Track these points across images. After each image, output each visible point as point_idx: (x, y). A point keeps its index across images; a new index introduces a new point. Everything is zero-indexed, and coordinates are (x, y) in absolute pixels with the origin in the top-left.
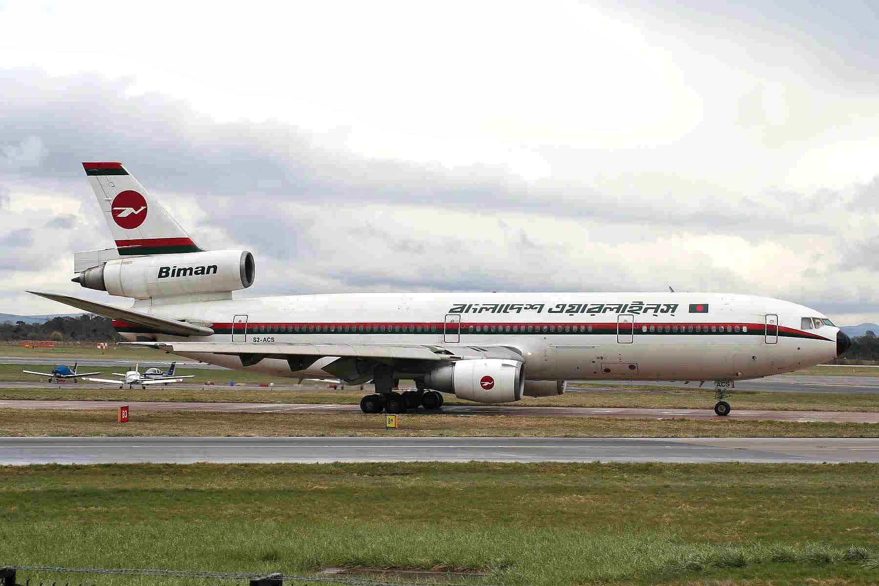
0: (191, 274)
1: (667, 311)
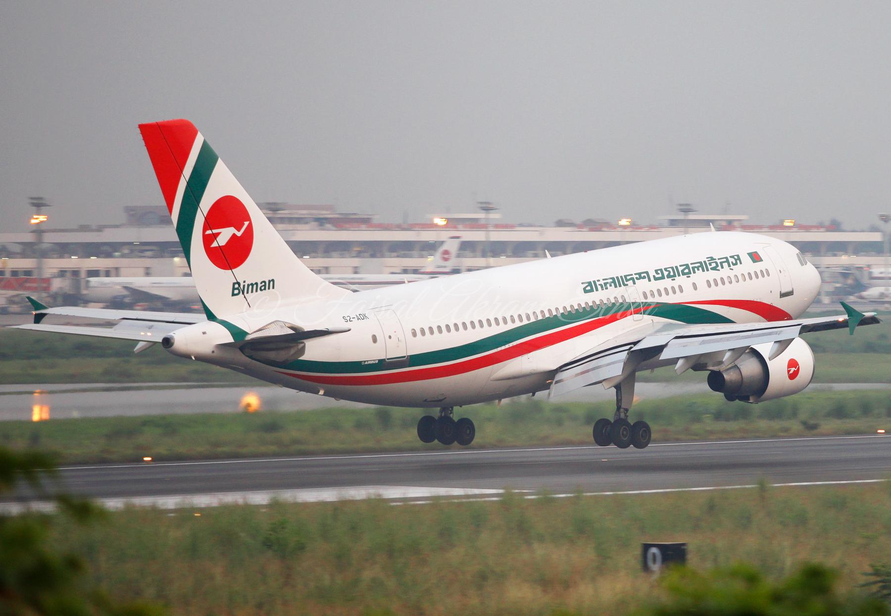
1: (736, 264)
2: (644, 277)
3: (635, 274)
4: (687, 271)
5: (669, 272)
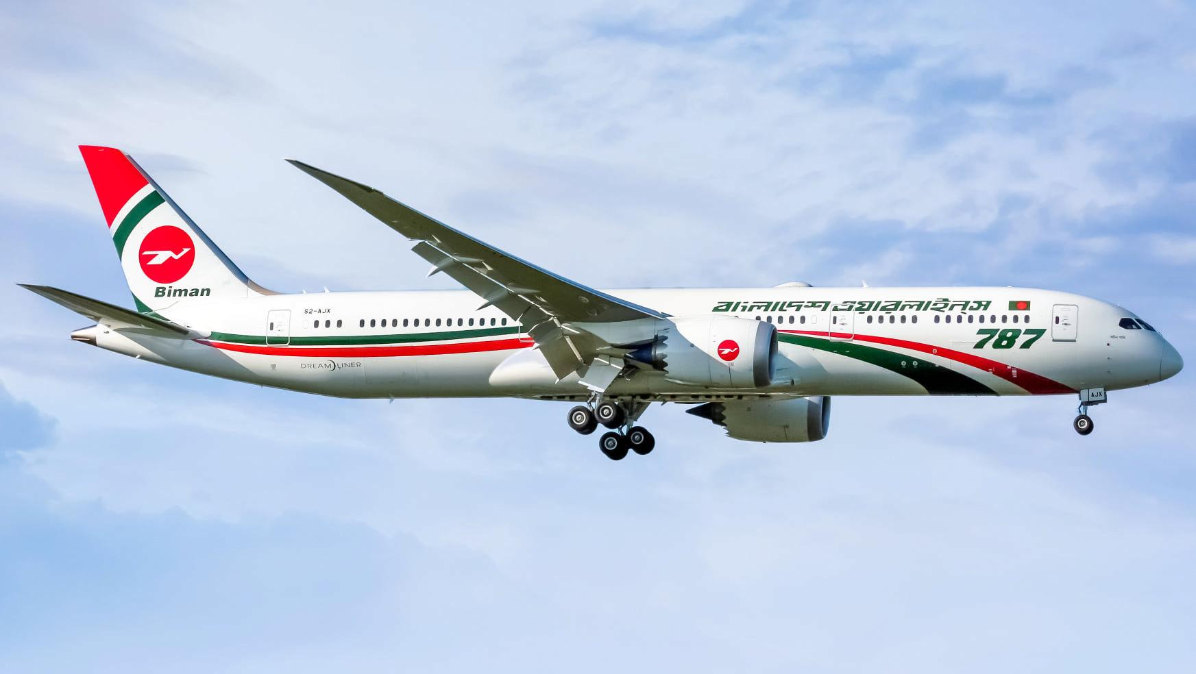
0: (186, 295)
1: (977, 309)
2: (820, 306)
3: (808, 302)
4: (893, 307)
5: (865, 305)
